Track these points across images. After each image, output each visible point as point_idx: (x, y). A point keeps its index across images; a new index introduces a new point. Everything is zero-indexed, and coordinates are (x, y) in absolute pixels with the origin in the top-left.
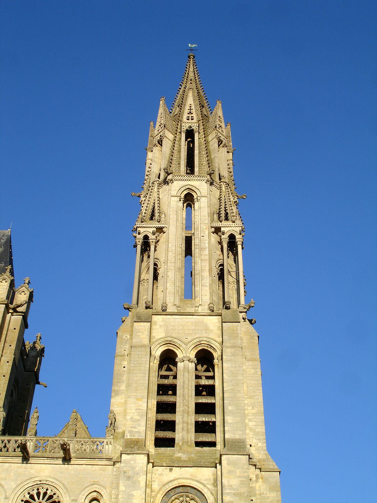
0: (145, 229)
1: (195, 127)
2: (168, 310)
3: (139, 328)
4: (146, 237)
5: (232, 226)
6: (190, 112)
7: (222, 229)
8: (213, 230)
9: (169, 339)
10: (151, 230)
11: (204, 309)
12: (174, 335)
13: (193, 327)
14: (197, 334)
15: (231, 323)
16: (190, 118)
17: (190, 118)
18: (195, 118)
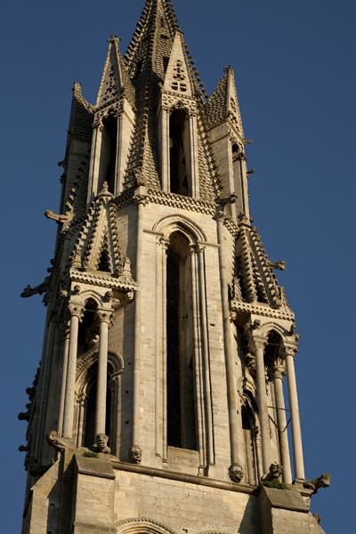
0: (88, 287)
1: (190, 105)
2: (142, 463)
3: (91, 487)
4: (91, 305)
5: (273, 314)
6: (179, 76)
7: (254, 318)
8: (234, 315)
9: (148, 524)
10: (103, 291)
11: (219, 472)
12: (158, 519)
13: (199, 509)
14: (208, 525)
15: (290, 512)
16: (179, 86)
17: (179, 86)
18: (188, 87)
